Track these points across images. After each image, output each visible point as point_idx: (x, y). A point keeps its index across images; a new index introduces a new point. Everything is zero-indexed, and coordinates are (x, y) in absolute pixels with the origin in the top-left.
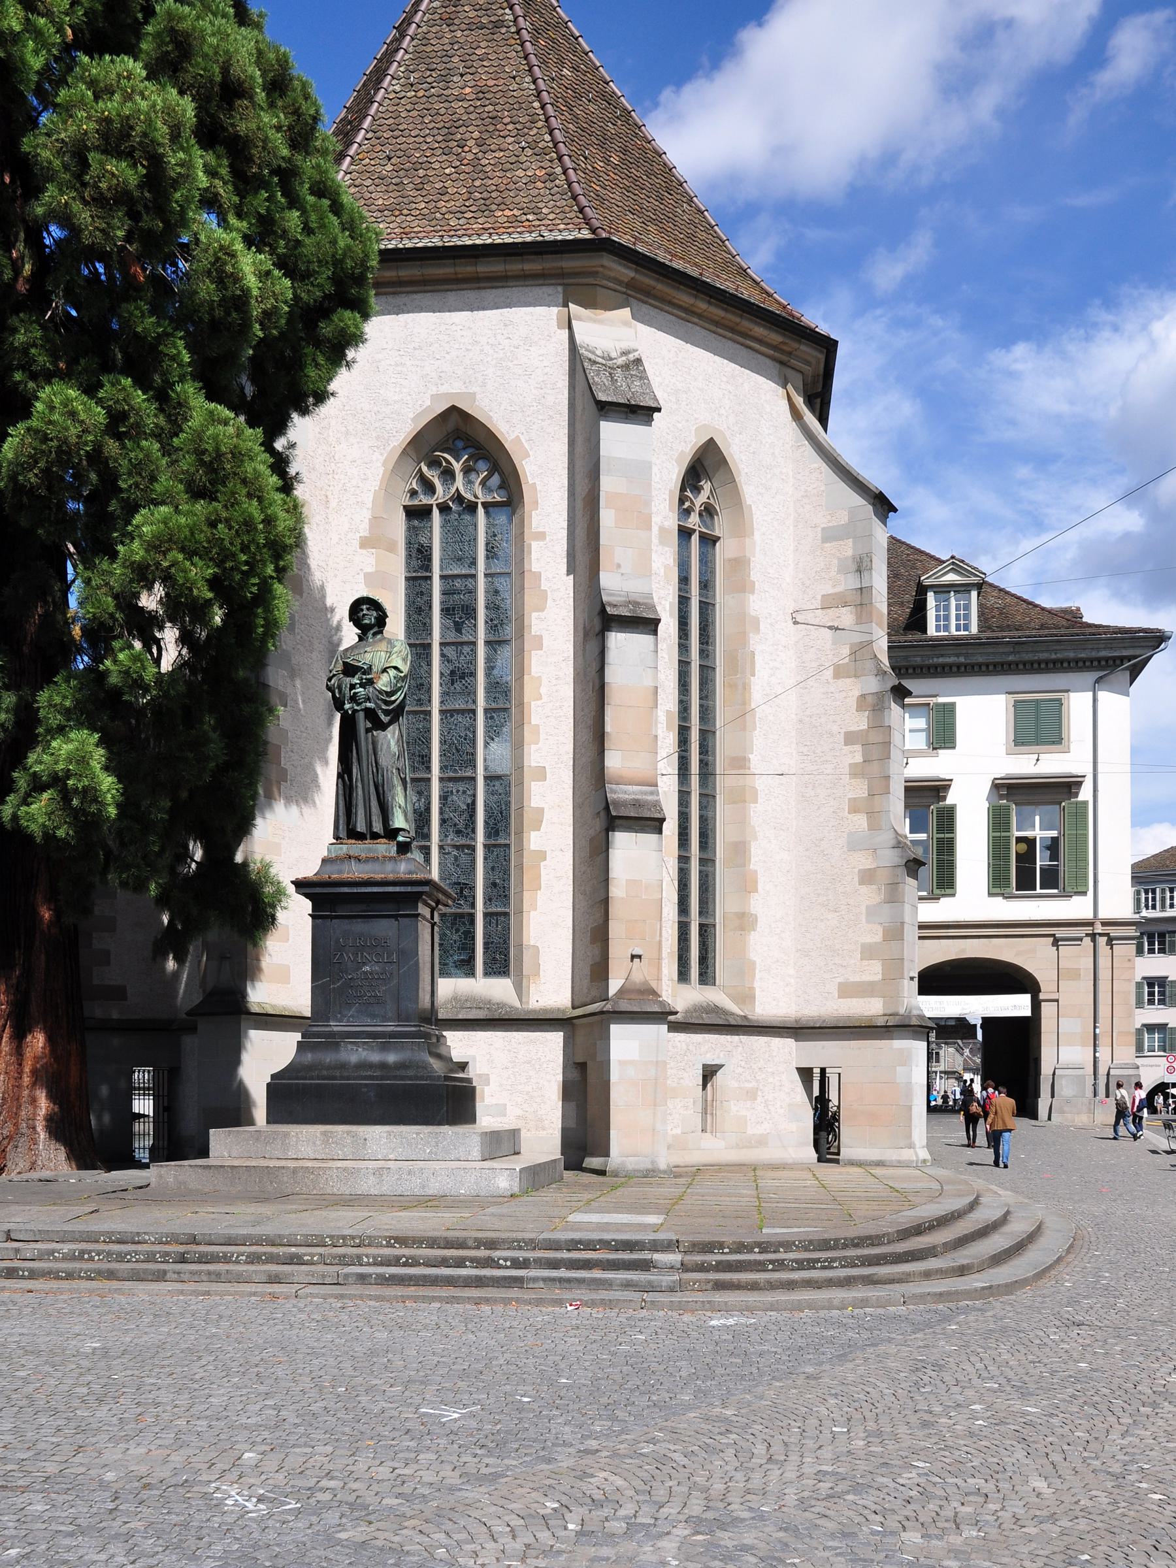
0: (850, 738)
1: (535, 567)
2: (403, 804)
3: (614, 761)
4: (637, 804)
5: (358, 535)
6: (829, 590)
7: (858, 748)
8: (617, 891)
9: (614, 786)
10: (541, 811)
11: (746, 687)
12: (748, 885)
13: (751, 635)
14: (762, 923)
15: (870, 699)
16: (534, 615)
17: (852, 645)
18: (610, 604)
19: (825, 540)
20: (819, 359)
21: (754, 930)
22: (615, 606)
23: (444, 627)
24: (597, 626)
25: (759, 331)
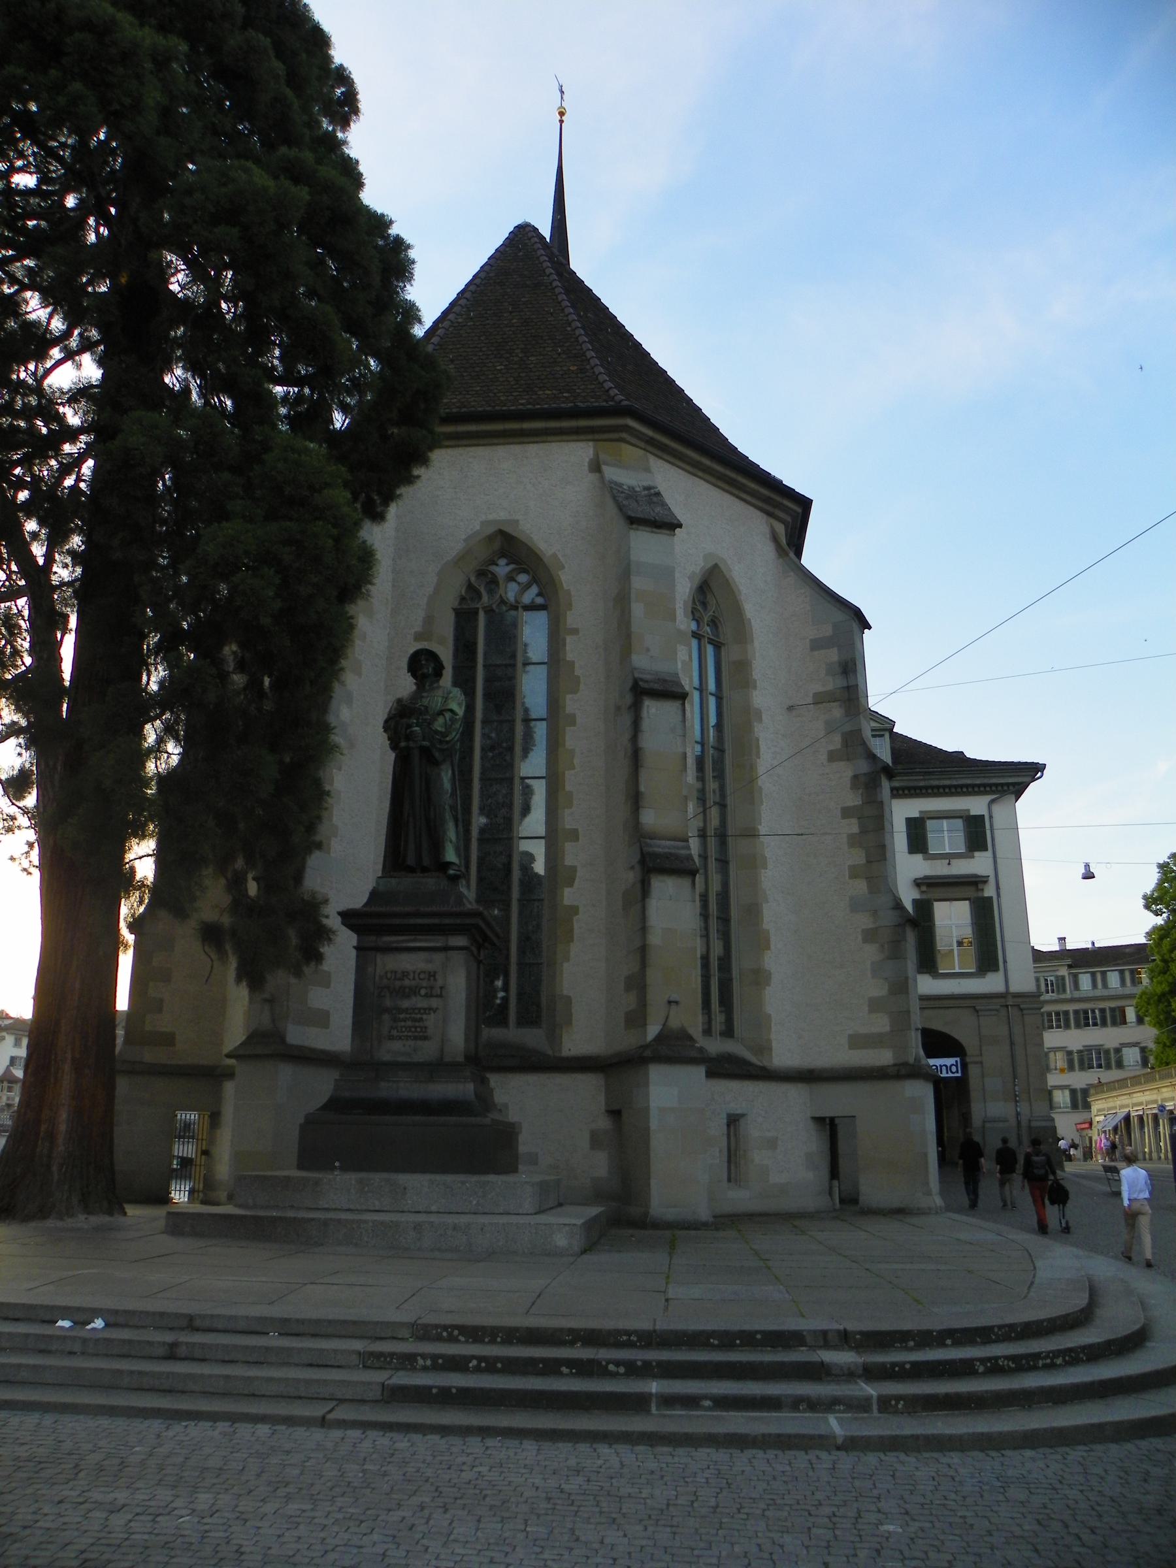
0: (846, 812)
1: (570, 656)
2: (454, 838)
3: (649, 818)
4: (668, 856)
5: (413, 631)
6: (819, 688)
7: (854, 821)
8: (654, 939)
9: (648, 841)
10: (573, 869)
11: (752, 767)
12: (761, 943)
13: (755, 724)
16: (569, 696)
18: (642, 680)
19: (813, 649)
20: (798, 513)
21: (769, 985)
22: (647, 681)
23: (486, 710)
24: (629, 699)
25: (752, 485)
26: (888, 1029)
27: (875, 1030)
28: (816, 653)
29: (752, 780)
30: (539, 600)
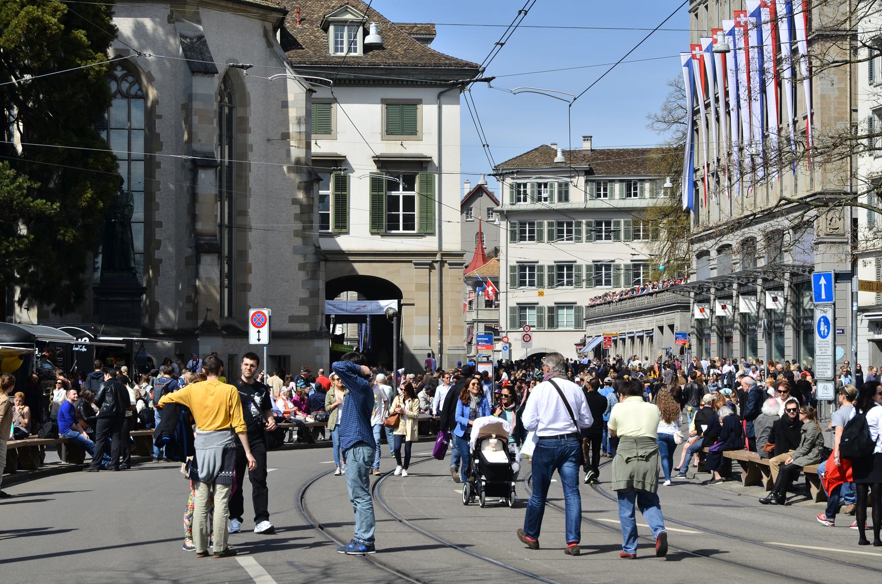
1: (157, 131)
3: (200, 226)
7: (298, 206)
10: (160, 241)
11: (247, 178)
26: (307, 314)
27: (302, 314)
29: (246, 184)
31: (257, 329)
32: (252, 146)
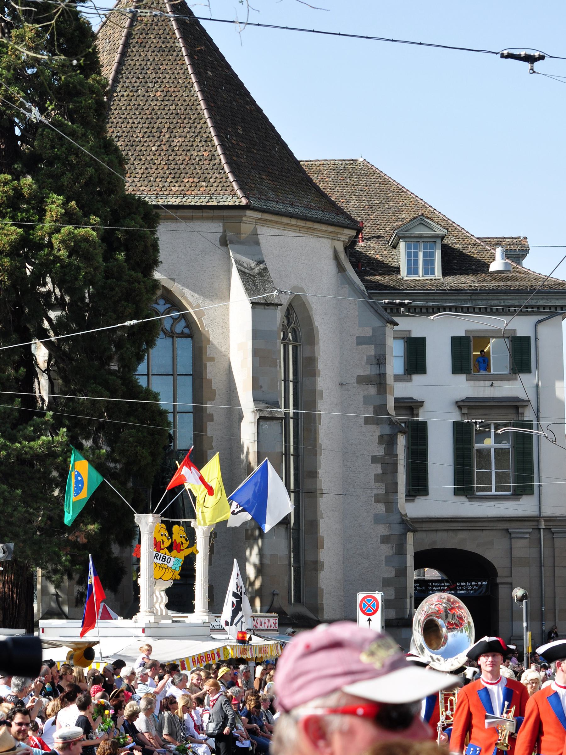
0: (374, 459)
1: (209, 376)
7: (379, 465)
14: (326, 567)
15: (386, 438)
17: (375, 407)
19: (359, 343)
28: (360, 347)
30: (187, 331)
31: (368, 617)
32: (321, 392)
